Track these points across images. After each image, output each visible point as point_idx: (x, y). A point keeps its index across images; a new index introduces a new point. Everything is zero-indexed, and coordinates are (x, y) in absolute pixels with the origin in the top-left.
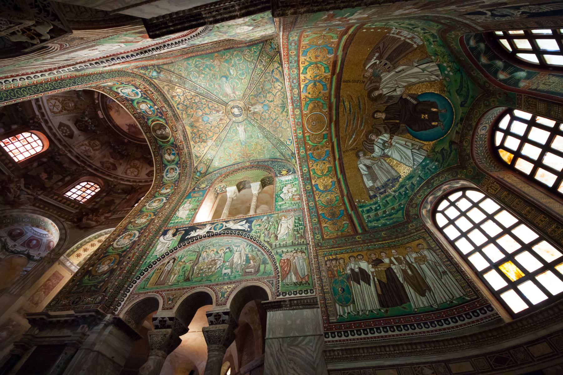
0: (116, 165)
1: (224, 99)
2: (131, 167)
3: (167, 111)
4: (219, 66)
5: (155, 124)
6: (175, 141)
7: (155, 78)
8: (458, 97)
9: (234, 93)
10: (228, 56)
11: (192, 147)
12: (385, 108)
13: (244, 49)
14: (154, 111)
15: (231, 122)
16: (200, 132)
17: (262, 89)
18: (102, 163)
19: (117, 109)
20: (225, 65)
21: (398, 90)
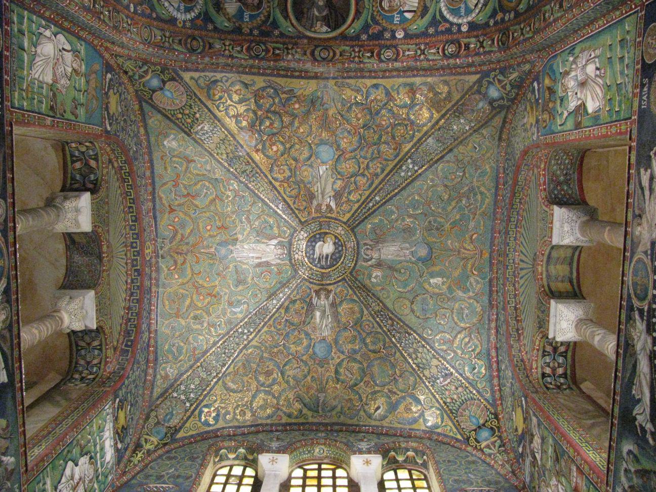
3: (381, 61)
4: (459, 251)
6: (282, 35)
7: (479, 81)
9: (379, 264)
11: (247, 78)
13: (484, 337)
17: (374, 352)
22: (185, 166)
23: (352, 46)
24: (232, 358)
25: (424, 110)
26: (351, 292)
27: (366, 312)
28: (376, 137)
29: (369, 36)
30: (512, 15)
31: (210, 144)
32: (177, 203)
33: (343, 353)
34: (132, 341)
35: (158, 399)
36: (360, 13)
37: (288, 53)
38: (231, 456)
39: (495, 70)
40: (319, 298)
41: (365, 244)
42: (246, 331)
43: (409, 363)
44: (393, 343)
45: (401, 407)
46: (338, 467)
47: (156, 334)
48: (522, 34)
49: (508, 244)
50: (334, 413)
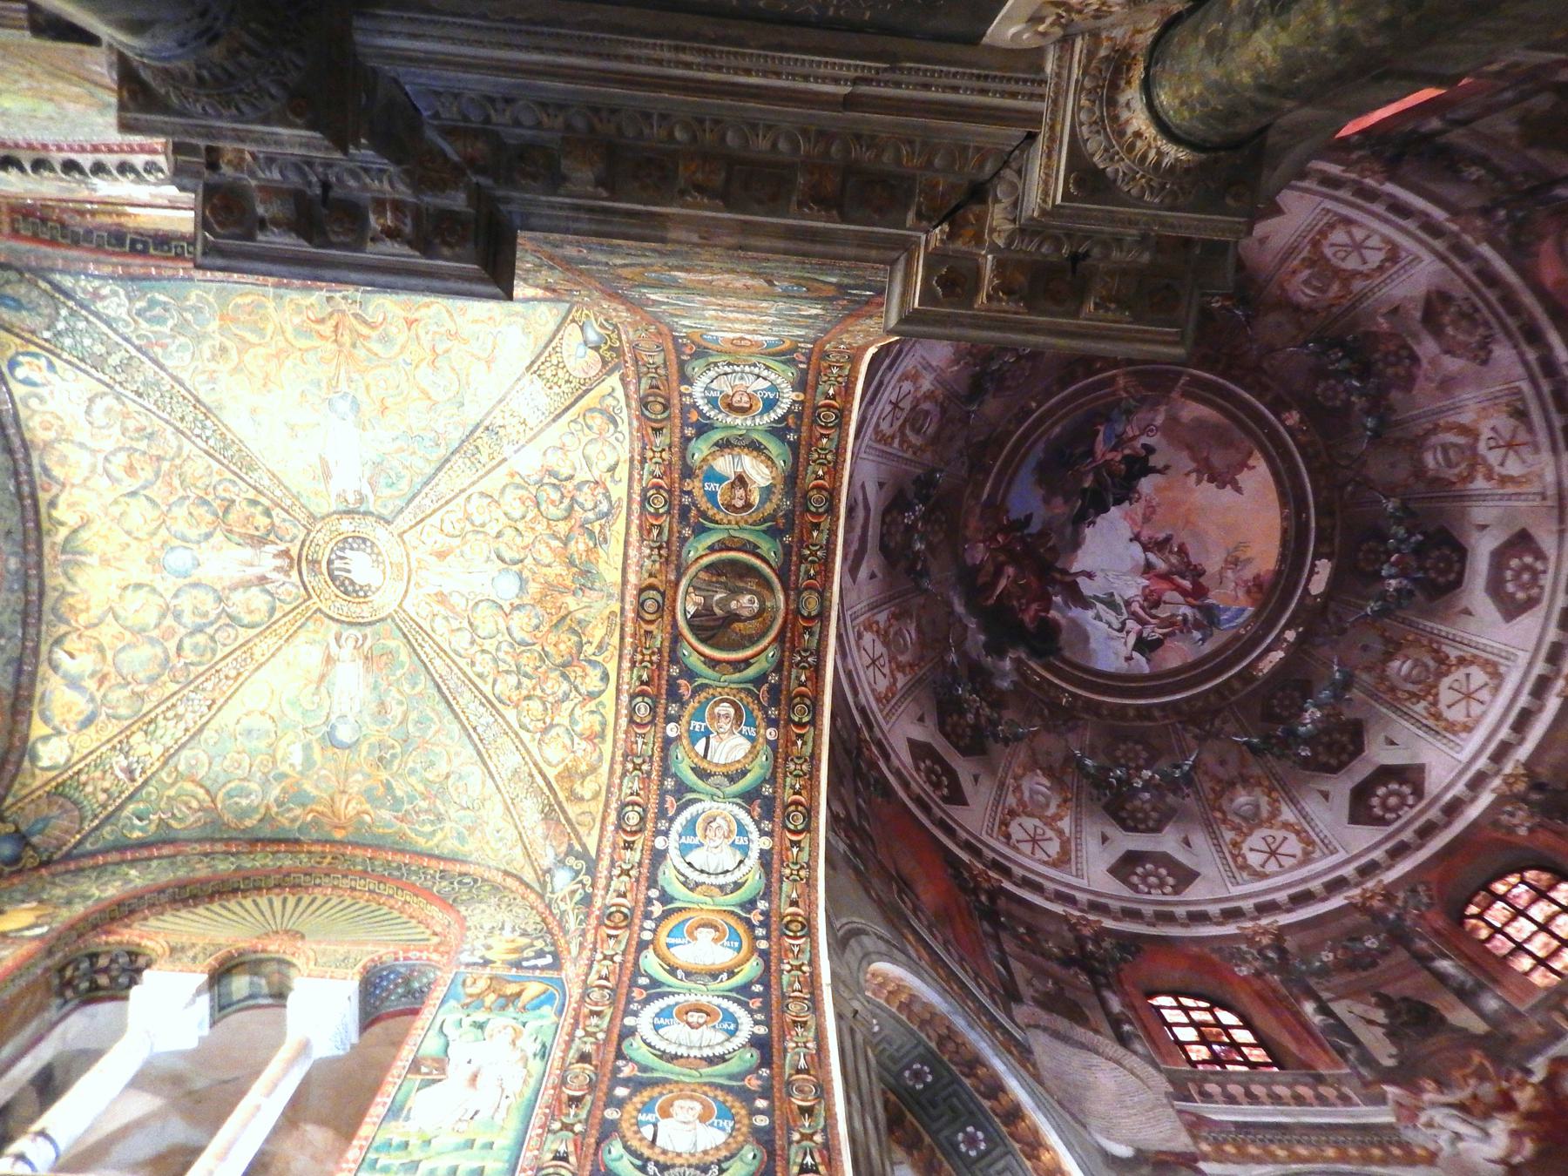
0: (1418, 315)
2: (1347, 277)
3: (632, 697)
4: (344, 792)
5: (744, 647)
6: (684, 540)
7: (583, 855)
10: (291, 815)
11: (623, 472)
13: (195, 835)
14: (698, 715)
15: (402, 523)
16: (562, 527)
17: (179, 648)
18: (1482, 354)
19: (1229, 574)
20: (317, 787)
23: (660, 651)
24: (154, 409)
25: (564, 754)
26: (288, 608)
28: (529, 670)
30: (647, 936)
32: (421, 332)
33: (176, 596)
35: (50, 282)
36: (713, 667)
37: (652, 549)
39: (593, 886)
40: (275, 556)
41: (365, 637)
42: (208, 433)
44: (197, 677)
47: (183, 279)
48: (605, 957)
49: (345, 876)
50: (62, 580)
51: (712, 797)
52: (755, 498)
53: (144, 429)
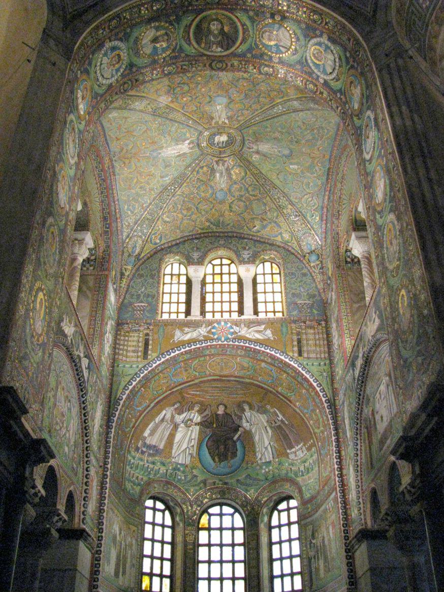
1: (251, 131)
3: (260, 73)
6: (187, 56)
8: (244, 476)
9: (258, 152)
10: (318, 170)
12: (229, 412)
15: (200, 128)
20: (307, 162)
21: (248, 424)
22: (124, 120)
23: (240, 61)
26: (239, 161)
27: (248, 173)
28: (256, 95)
29: (252, 56)
31: (141, 108)
33: (234, 197)
34: (109, 224)
36: (247, 40)
37: (192, 67)
38: (172, 260)
41: (248, 140)
43: (275, 204)
45: (269, 227)
46: (233, 262)
50: (229, 227)
51: (306, 51)
52: (163, 32)
53: (173, 206)
